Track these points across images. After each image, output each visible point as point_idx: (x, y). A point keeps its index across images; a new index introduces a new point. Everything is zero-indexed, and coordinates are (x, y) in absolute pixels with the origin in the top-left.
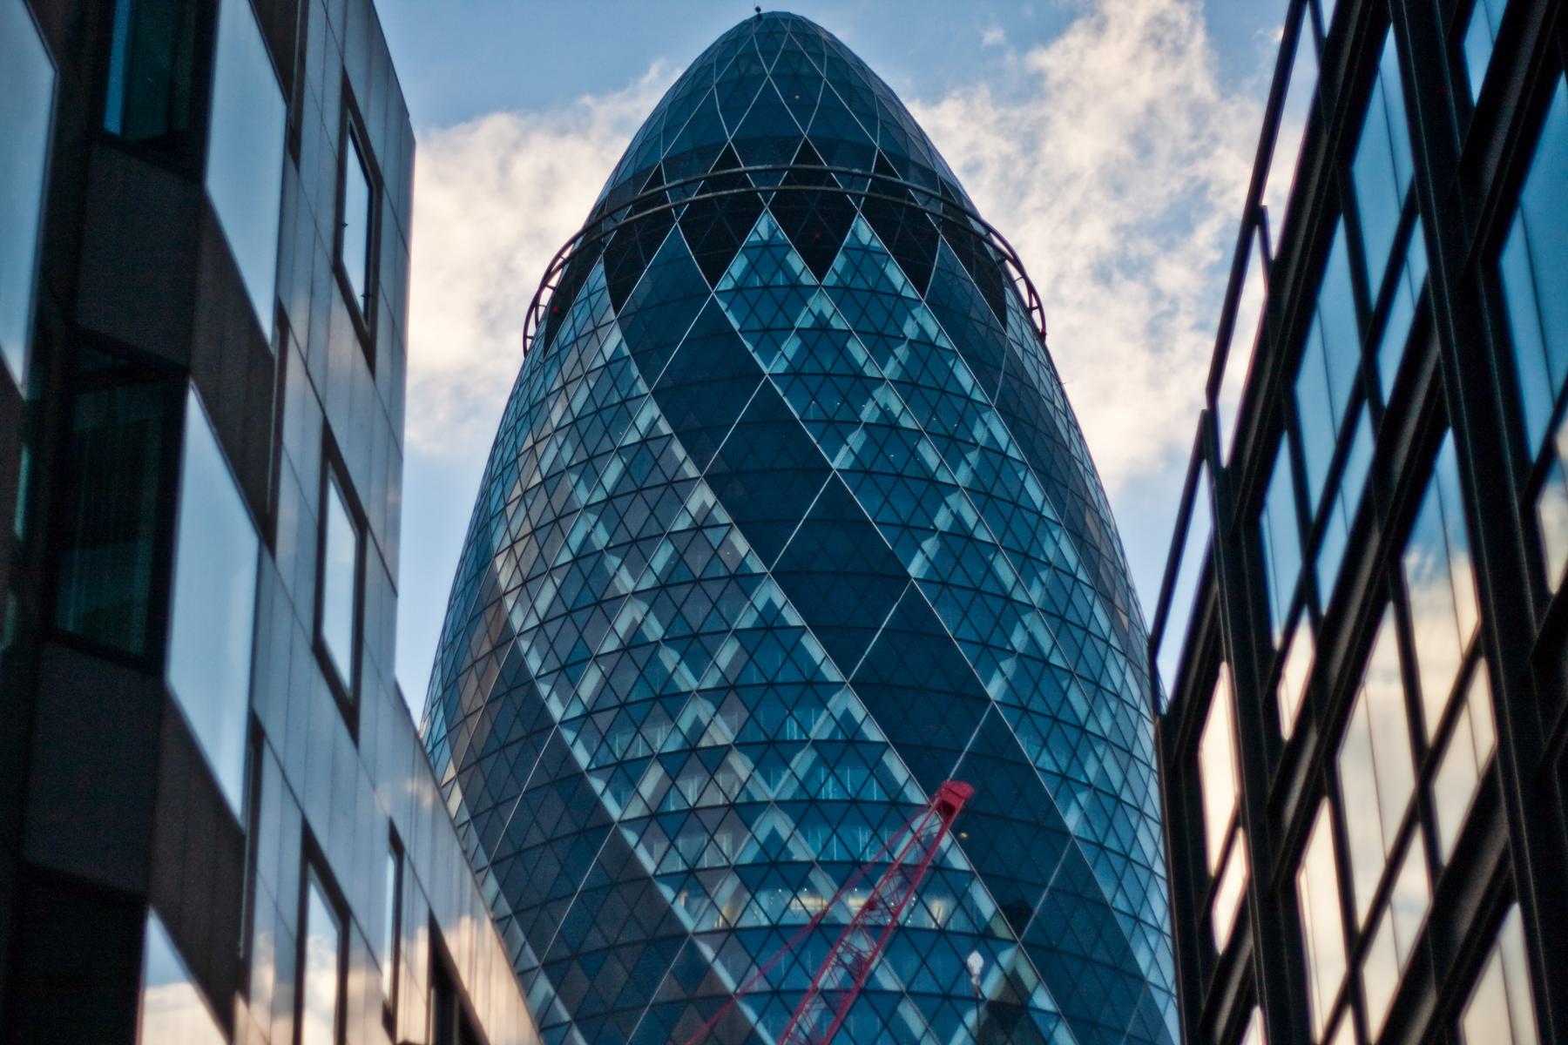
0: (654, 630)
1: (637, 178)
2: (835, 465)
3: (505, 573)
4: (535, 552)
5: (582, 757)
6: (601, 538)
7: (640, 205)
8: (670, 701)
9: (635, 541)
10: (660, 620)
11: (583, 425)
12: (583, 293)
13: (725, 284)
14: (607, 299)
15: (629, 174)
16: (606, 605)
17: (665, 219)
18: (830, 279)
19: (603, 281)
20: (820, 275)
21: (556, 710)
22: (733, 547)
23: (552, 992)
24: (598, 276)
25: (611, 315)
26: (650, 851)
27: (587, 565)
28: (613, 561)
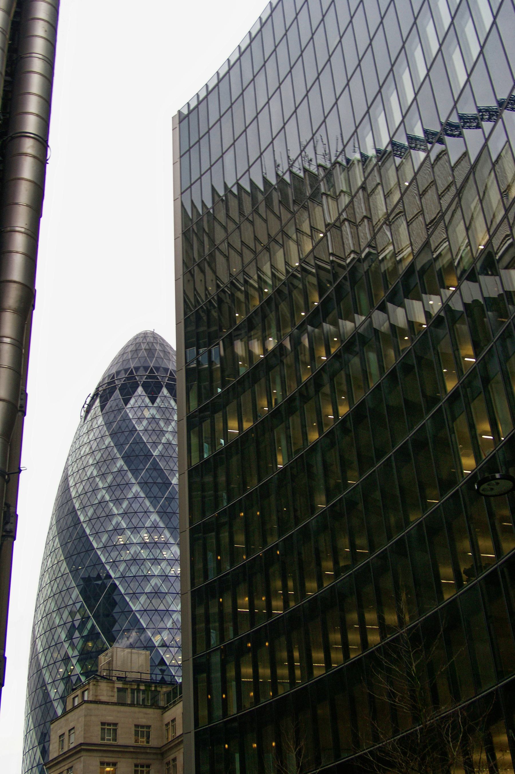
0: (107, 498)
1: (109, 376)
2: (154, 454)
3: (71, 483)
4: (78, 476)
5: (88, 531)
6: (95, 473)
7: (109, 383)
8: (110, 516)
9: (103, 474)
10: (109, 495)
11: (92, 442)
12: (94, 407)
13: (129, 406)
14: (99, 409)
15: (107, 375)
16: (95, 490)
17: (115, 388)
18: (156, 405)
19: (99, 404)
20: (153, 403)
21: (82, 518)
22: (128, 476)
23: (78, 593)
24: (97, 403)
25: (100, 414)
26: (104, 556)
27: (91, 480)
28: (97, 479)
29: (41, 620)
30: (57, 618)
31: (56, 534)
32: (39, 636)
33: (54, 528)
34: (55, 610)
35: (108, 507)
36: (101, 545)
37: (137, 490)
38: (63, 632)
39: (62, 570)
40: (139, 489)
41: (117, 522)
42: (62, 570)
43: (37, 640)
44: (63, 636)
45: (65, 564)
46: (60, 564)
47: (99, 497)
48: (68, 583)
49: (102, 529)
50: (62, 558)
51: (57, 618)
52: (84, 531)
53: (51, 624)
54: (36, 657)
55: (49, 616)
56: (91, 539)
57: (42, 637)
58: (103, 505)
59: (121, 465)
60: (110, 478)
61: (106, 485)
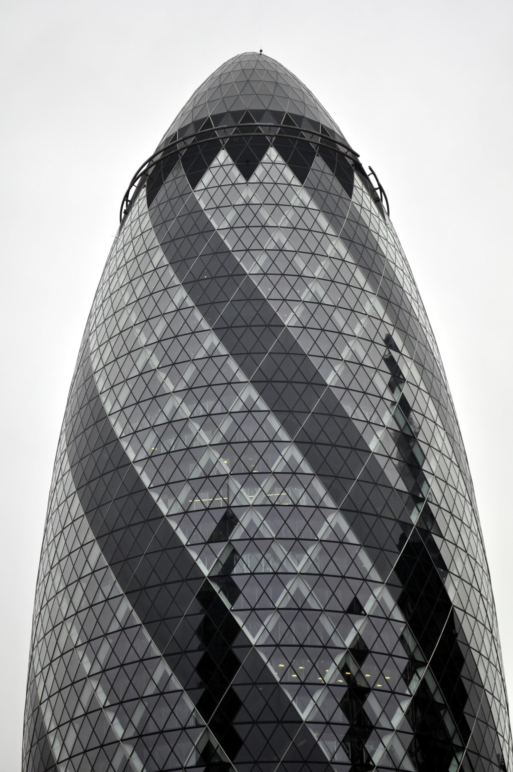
21: (131, 455)
23: (131, 608)
29: (50, 664)
30: (86, 659)
31: (74, 489)
32: (45, 697)
33: (69, 478)
34: (80, 643)
35: (189, 431)
36: (177, 509)
37: (250, 396)
38: (100, 689)
39: (93, 560)
40: (255, 395)
41: (210, 460)
42: (93, 560)
43: (43, 707)
44: (102, 697)
45: (97, 550)
46: (87, 548)
47: (168, 409)
48: (107, 589)
49: (178, 476)
50: (91, 536)
51: (86, 659)
52: (138, 479)
53: (72, 672)
54: (42, 742)
55: (67, 657)
56: (155, 496)
57: (53, 699)
58: (178, 426)
59: (212, 344)
60: (189, 373)
61: (182, 386)
